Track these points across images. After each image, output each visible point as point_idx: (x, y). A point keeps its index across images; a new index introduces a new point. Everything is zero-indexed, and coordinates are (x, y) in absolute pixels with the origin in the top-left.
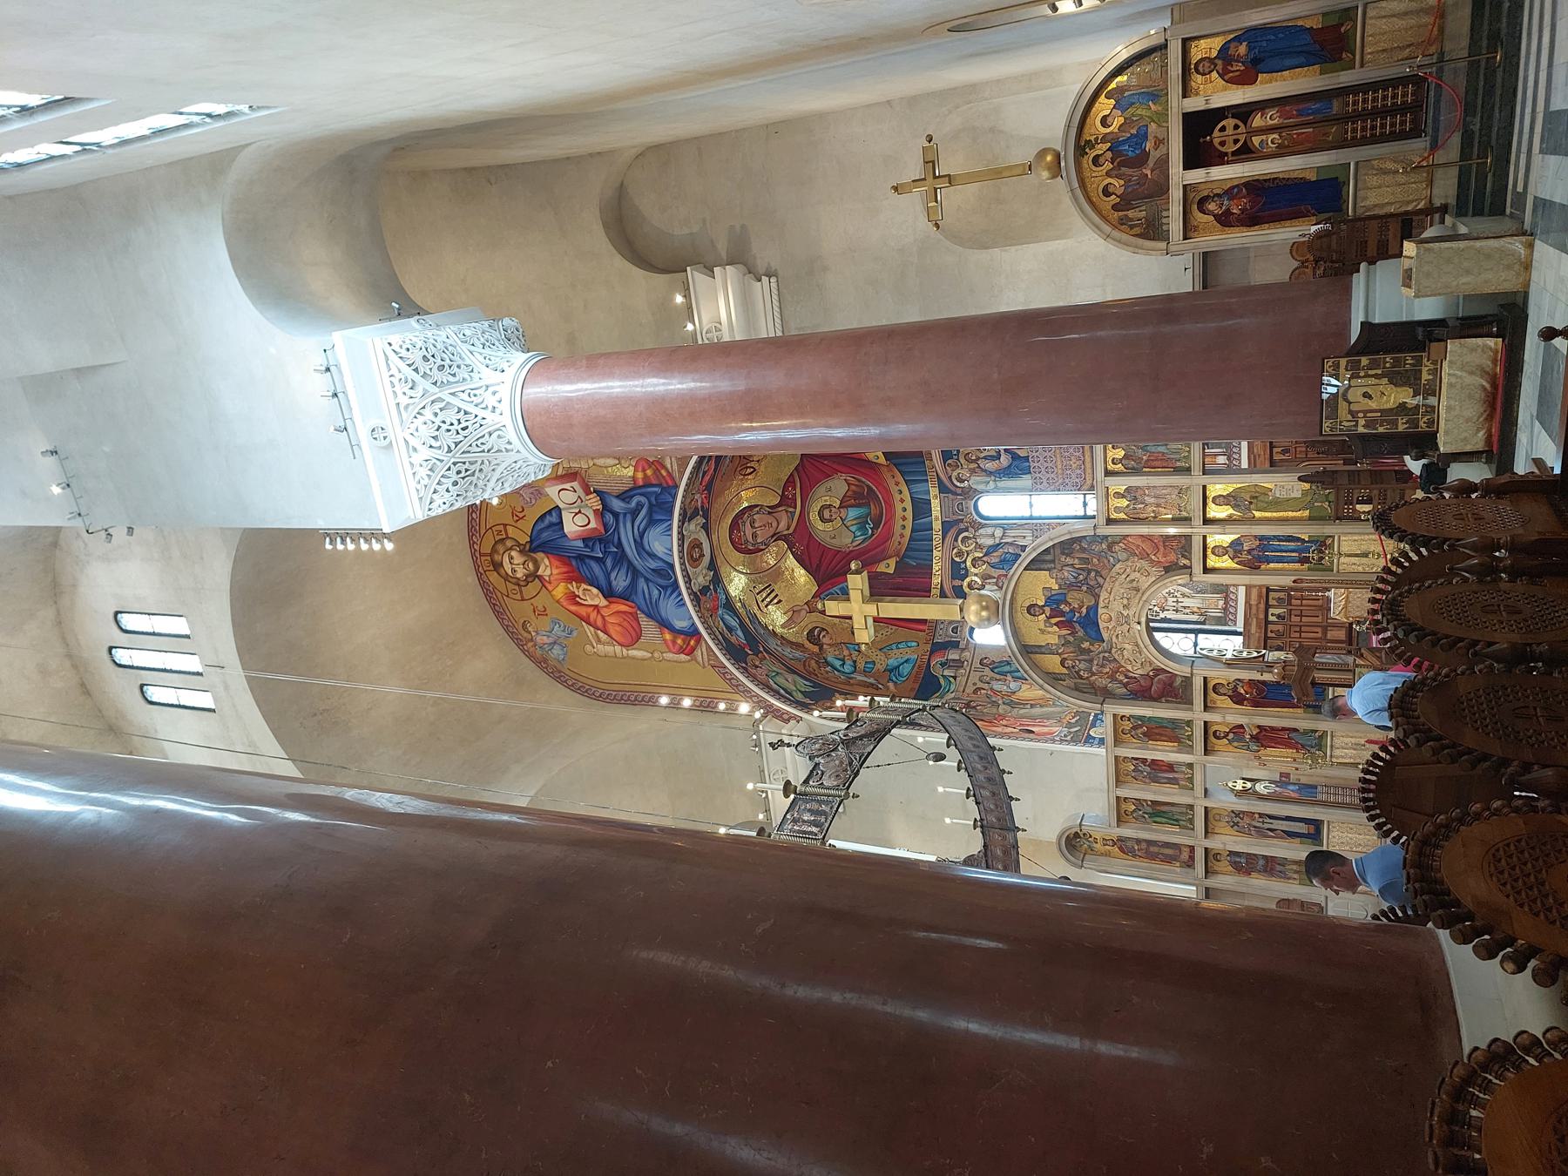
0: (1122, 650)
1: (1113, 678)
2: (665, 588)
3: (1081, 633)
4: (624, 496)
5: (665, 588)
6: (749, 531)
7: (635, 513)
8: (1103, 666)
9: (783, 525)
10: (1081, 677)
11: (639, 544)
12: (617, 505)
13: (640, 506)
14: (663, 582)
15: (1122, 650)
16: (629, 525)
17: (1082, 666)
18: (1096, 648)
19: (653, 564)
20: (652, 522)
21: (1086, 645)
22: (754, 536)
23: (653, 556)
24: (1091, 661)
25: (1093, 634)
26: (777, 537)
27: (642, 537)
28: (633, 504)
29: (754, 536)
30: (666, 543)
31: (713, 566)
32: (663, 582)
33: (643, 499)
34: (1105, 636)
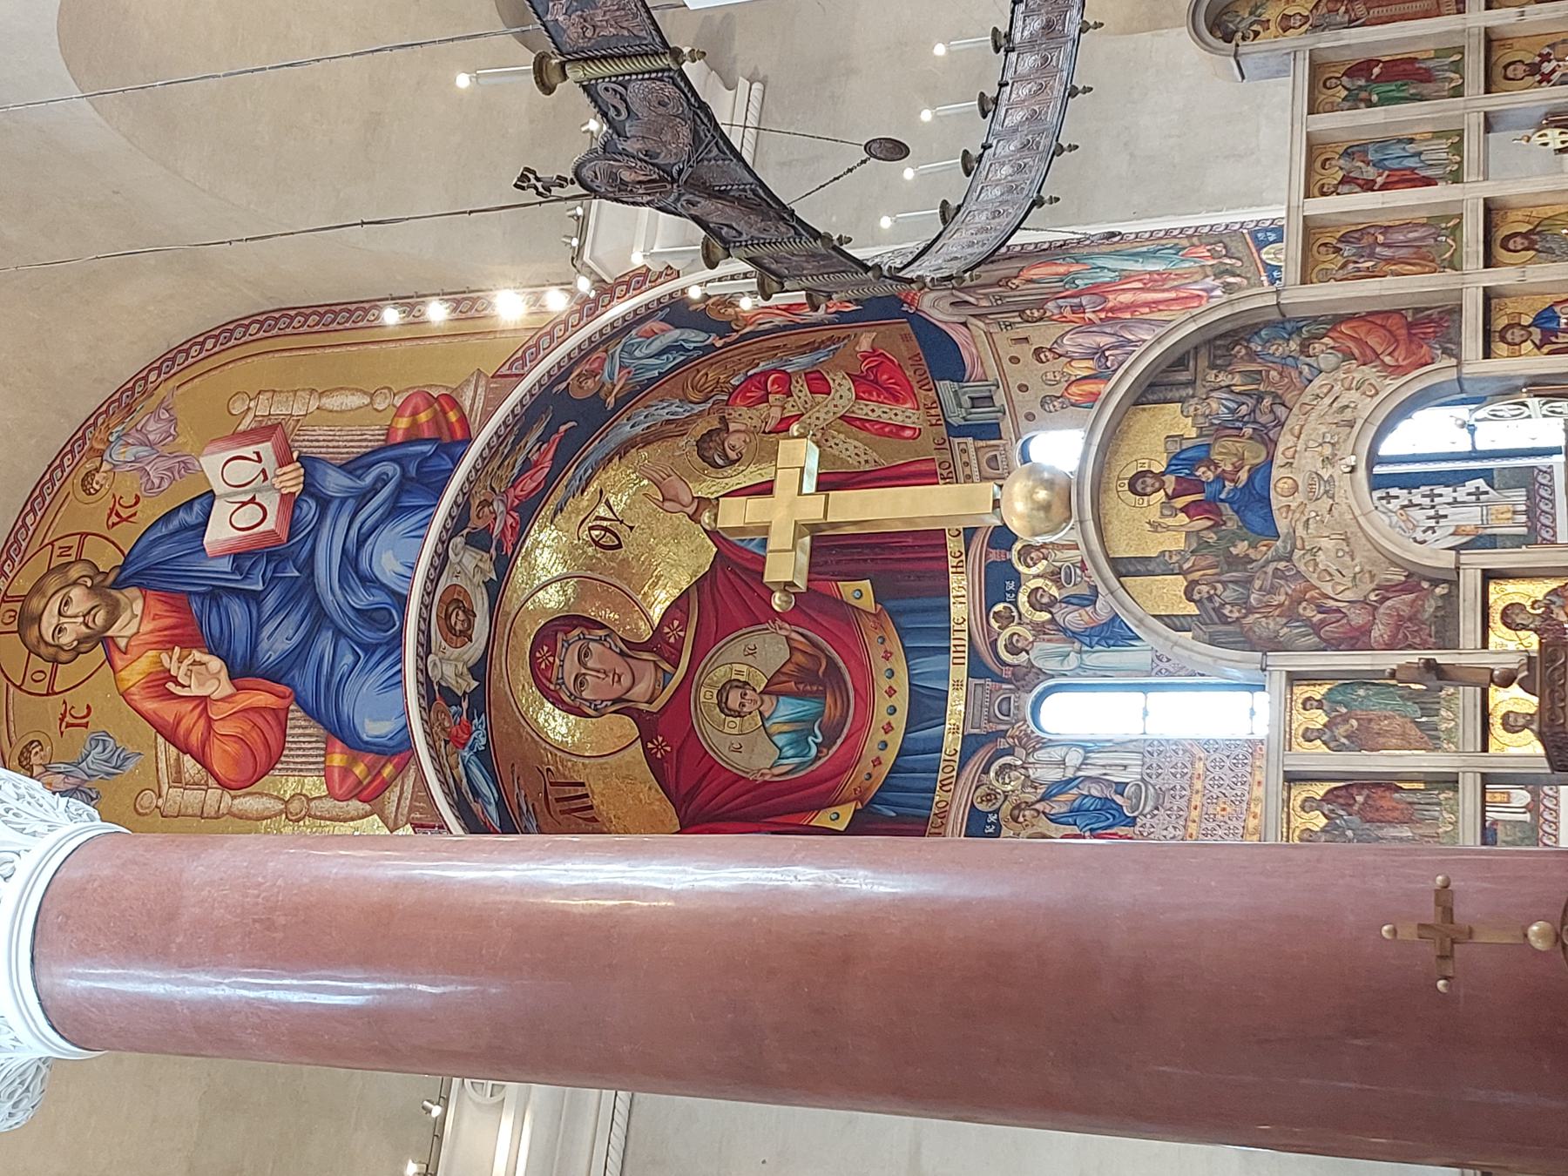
0: (1315, 551)
1: (1290, 614)
2: (369, 649)
3: (1232, 524)
4: (353, 467)
5: (369, 649)
6: (571, 668)
7: (364, 497)
8: (1273, 590)
9: (642, 689)
10: (1224, 620)
11: (350, 561)
12: (334, 483)
13: (382, 480)
14: (369, 636)
15: (1315, 551)
16: (344, 521)
17: (1229, 595)
18: (1262, 552)
19: (363, 599)
20: (395, 511)
21: (1241, 548)
22: (580, 681)
23: (370, 581)
24: (1247, 583)
25: (1257, 522)
26: (623, 706)
27: (361, 543)
28: (369, 479)
29: (580, 681)
30: (407, 557)
31: (480, 670)
32: (369, 636)
33: (391, 469)
34: (1282, 525)
